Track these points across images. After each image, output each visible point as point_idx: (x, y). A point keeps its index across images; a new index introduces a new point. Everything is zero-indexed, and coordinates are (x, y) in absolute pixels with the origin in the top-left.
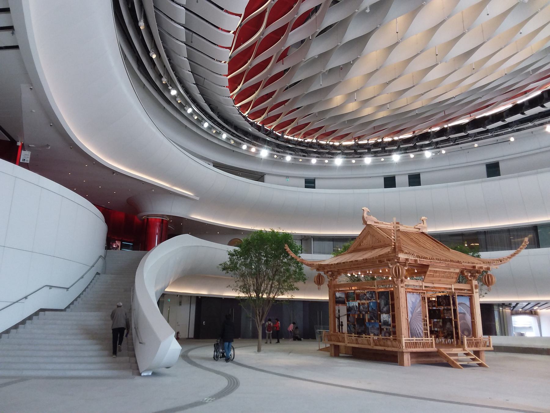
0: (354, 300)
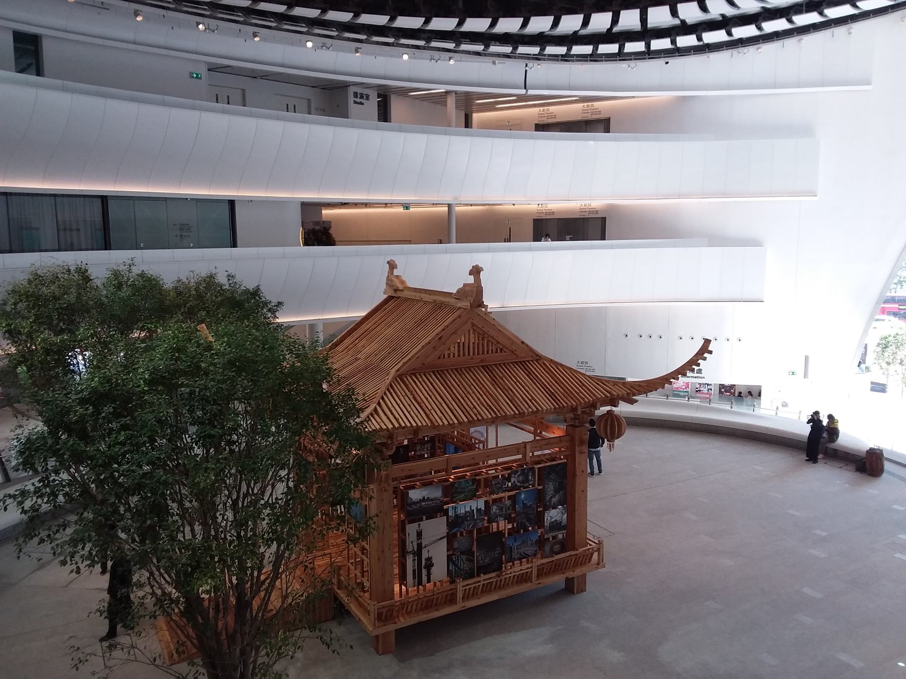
0: (473, 496)
